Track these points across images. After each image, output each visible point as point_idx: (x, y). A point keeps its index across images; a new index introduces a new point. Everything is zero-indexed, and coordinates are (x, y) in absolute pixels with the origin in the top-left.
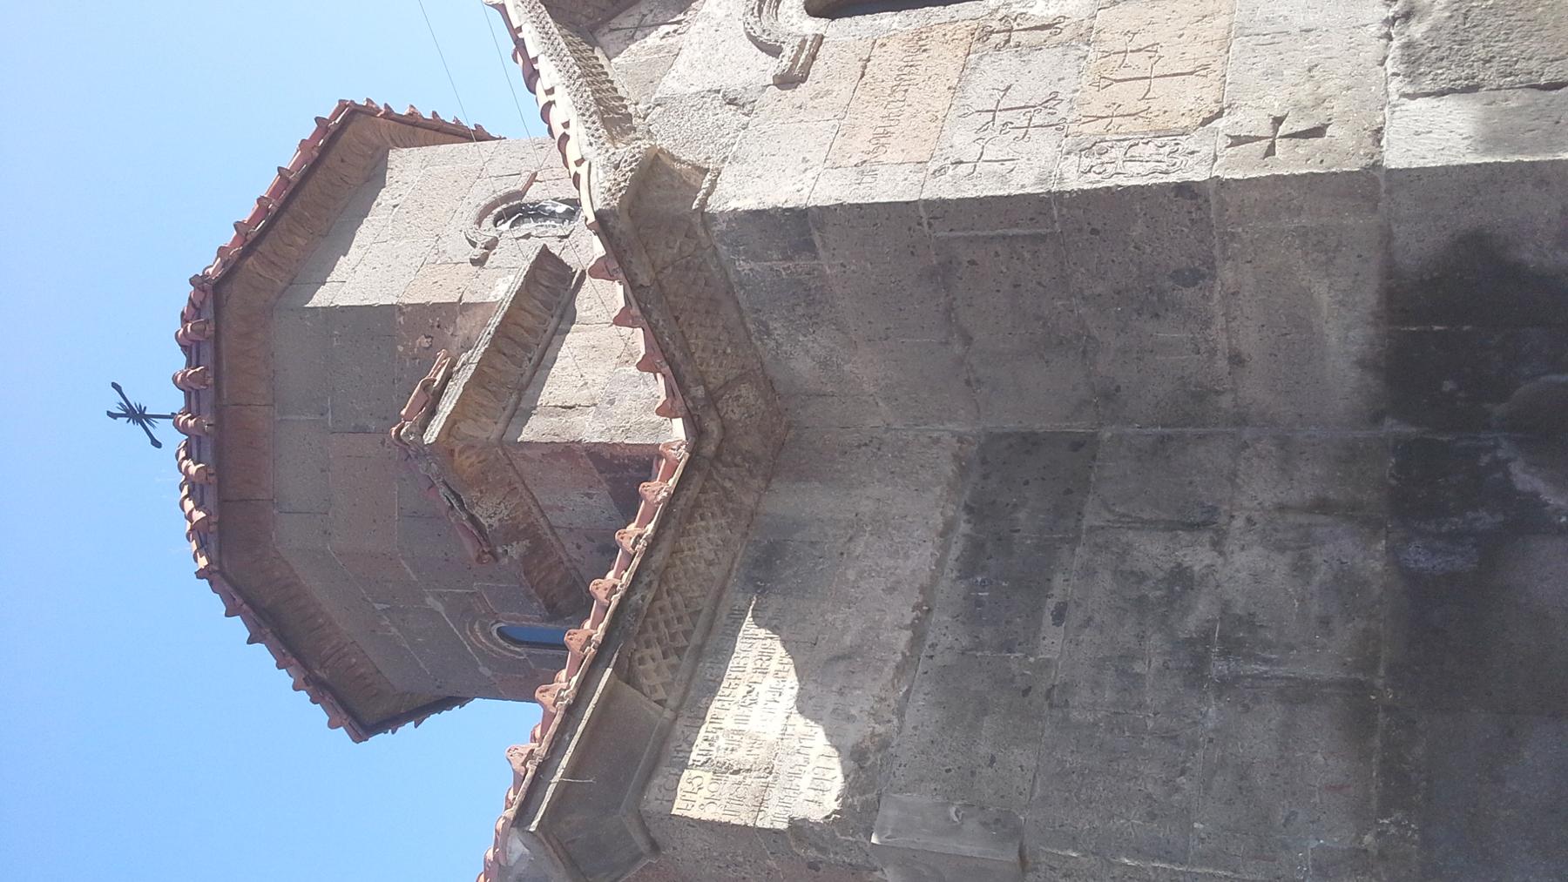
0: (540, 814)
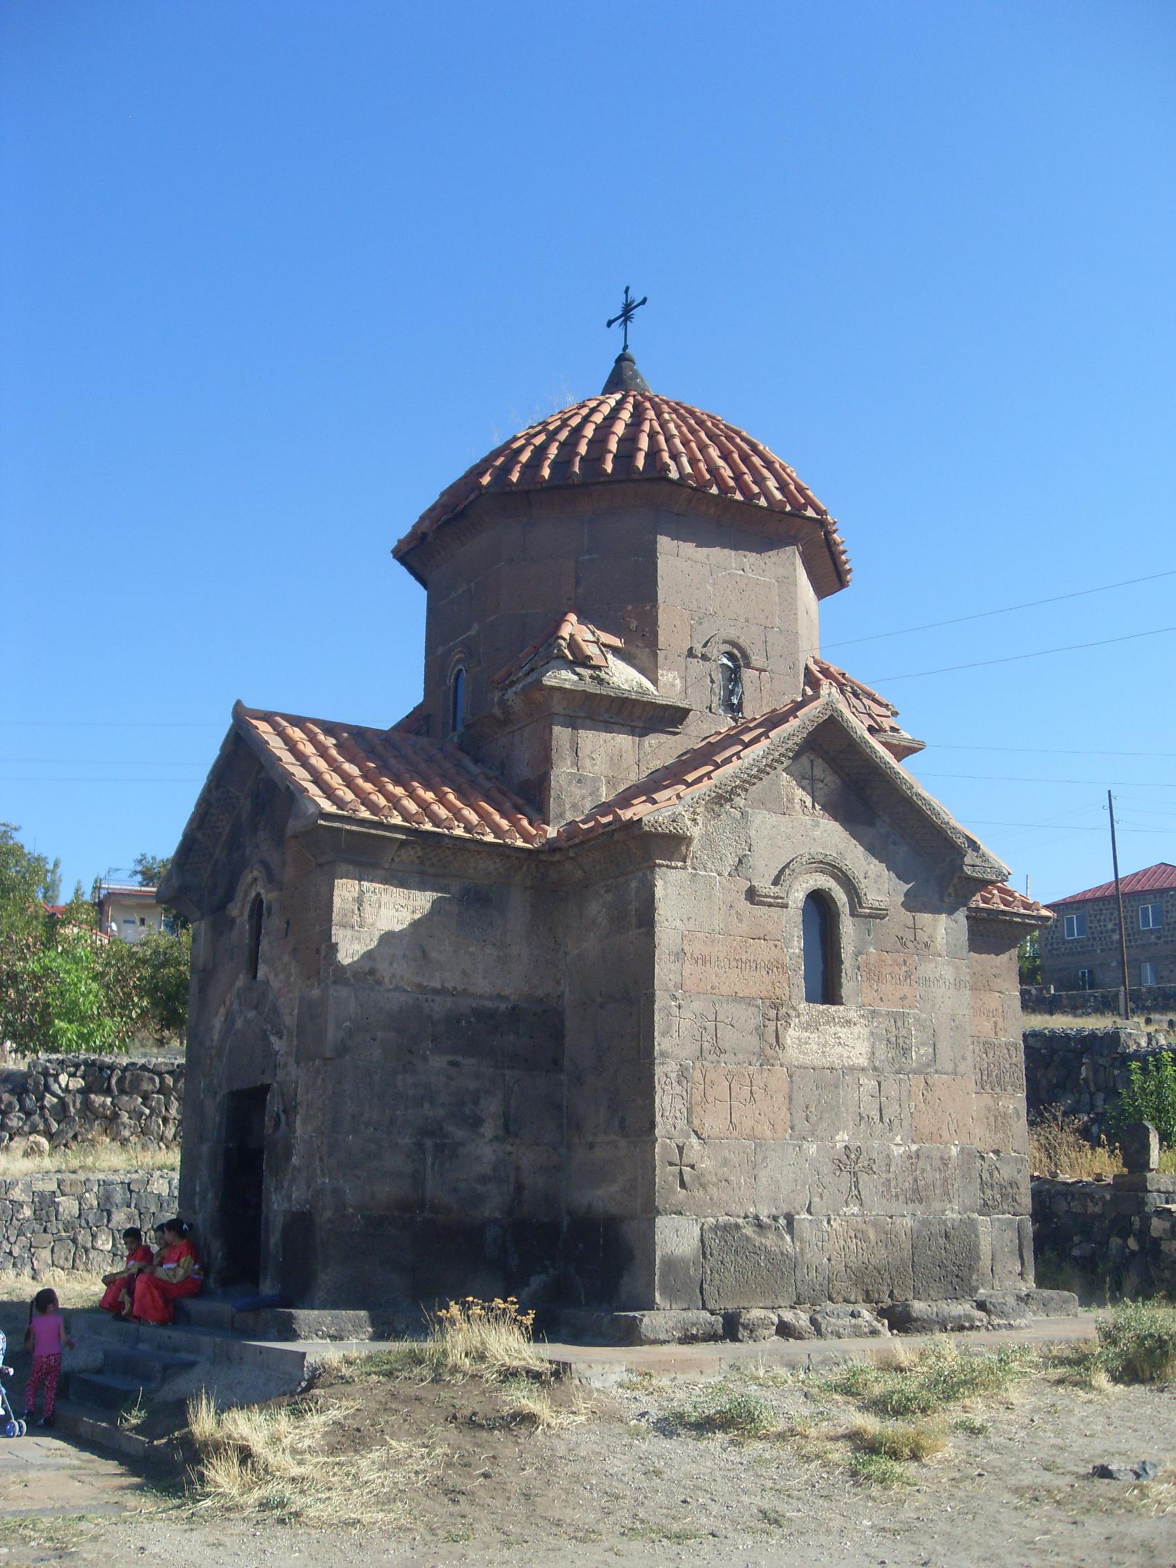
0: (326, 824)
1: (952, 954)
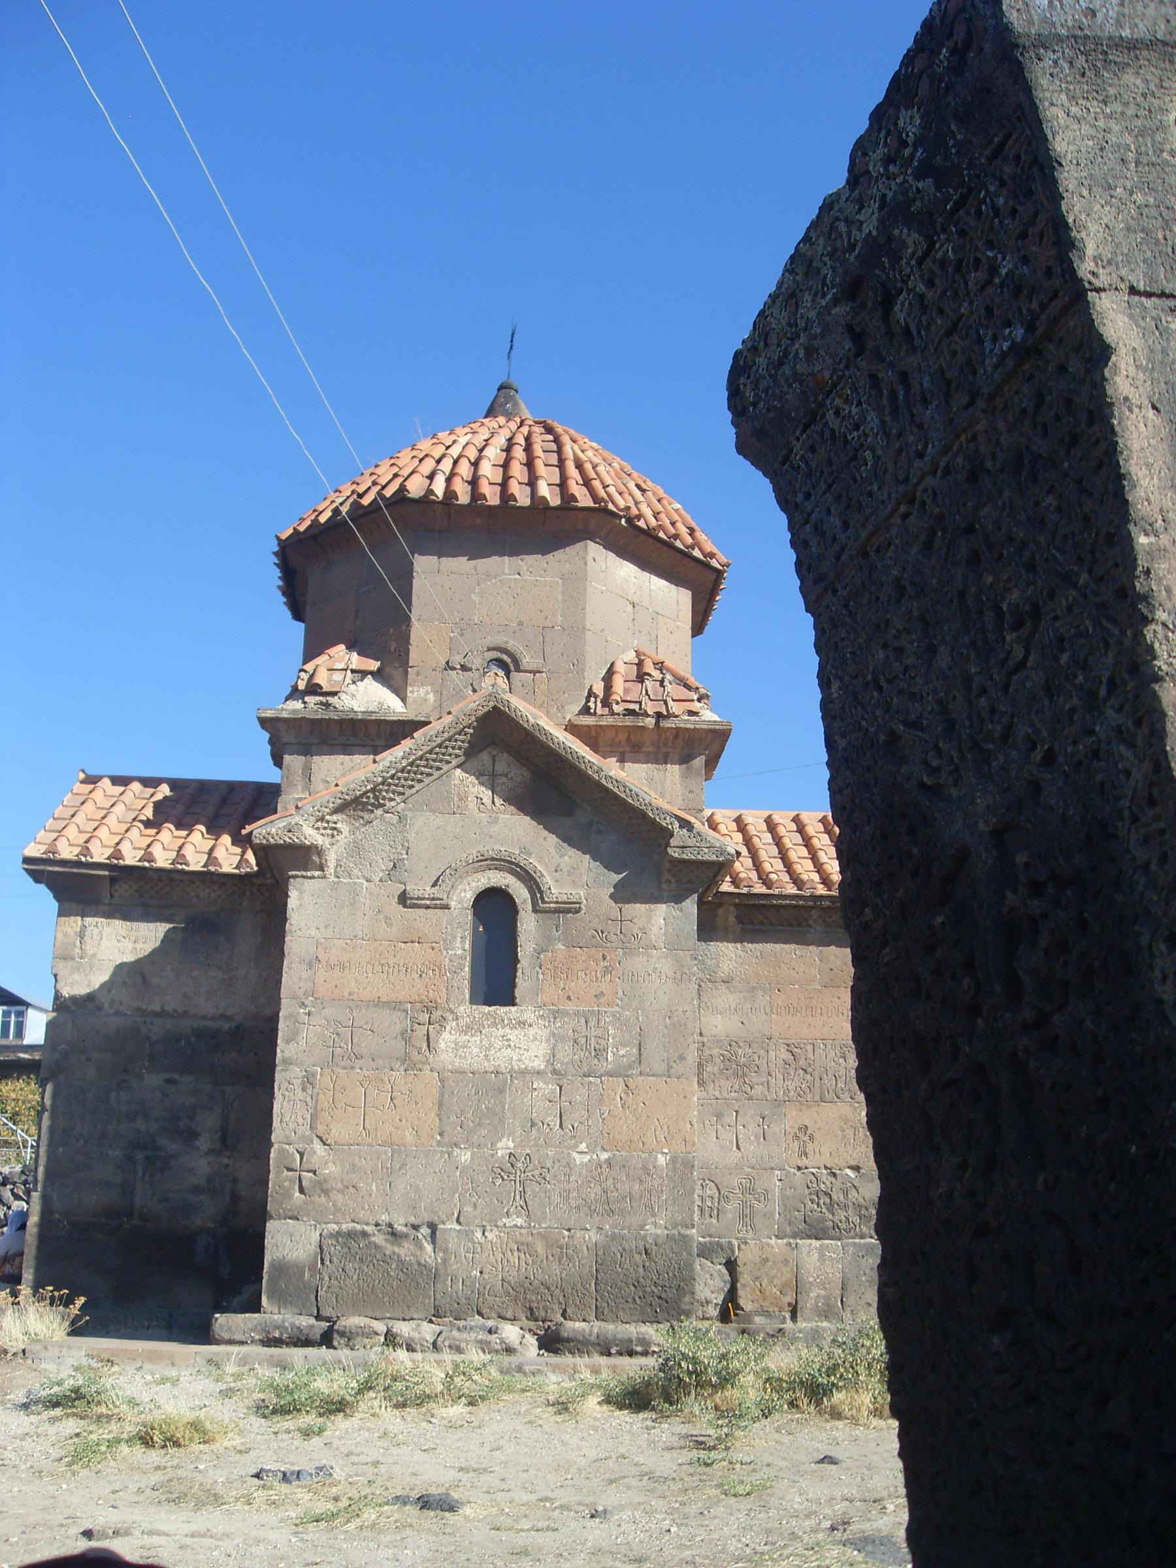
1: (673, 946)
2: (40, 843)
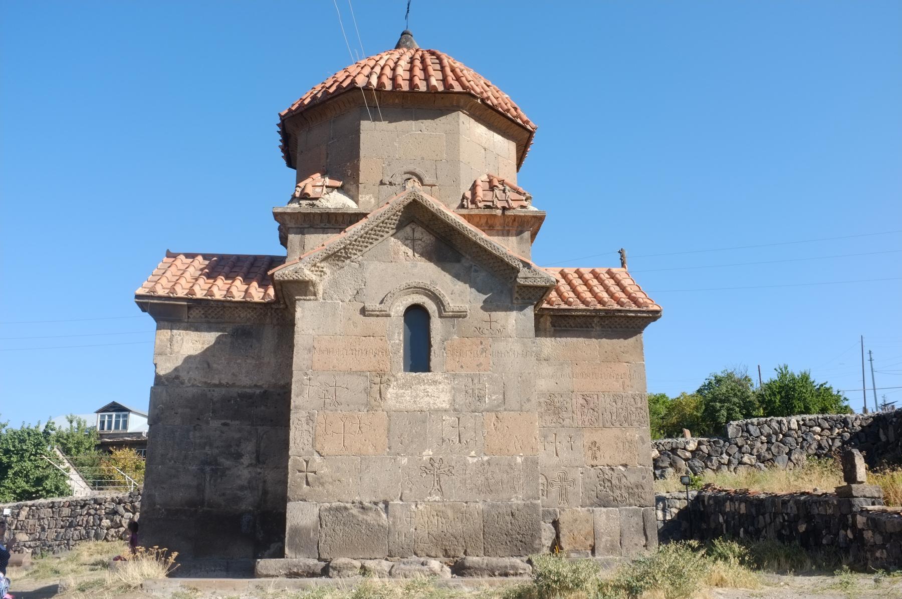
1: (521, 336)
2: (145, 288)
